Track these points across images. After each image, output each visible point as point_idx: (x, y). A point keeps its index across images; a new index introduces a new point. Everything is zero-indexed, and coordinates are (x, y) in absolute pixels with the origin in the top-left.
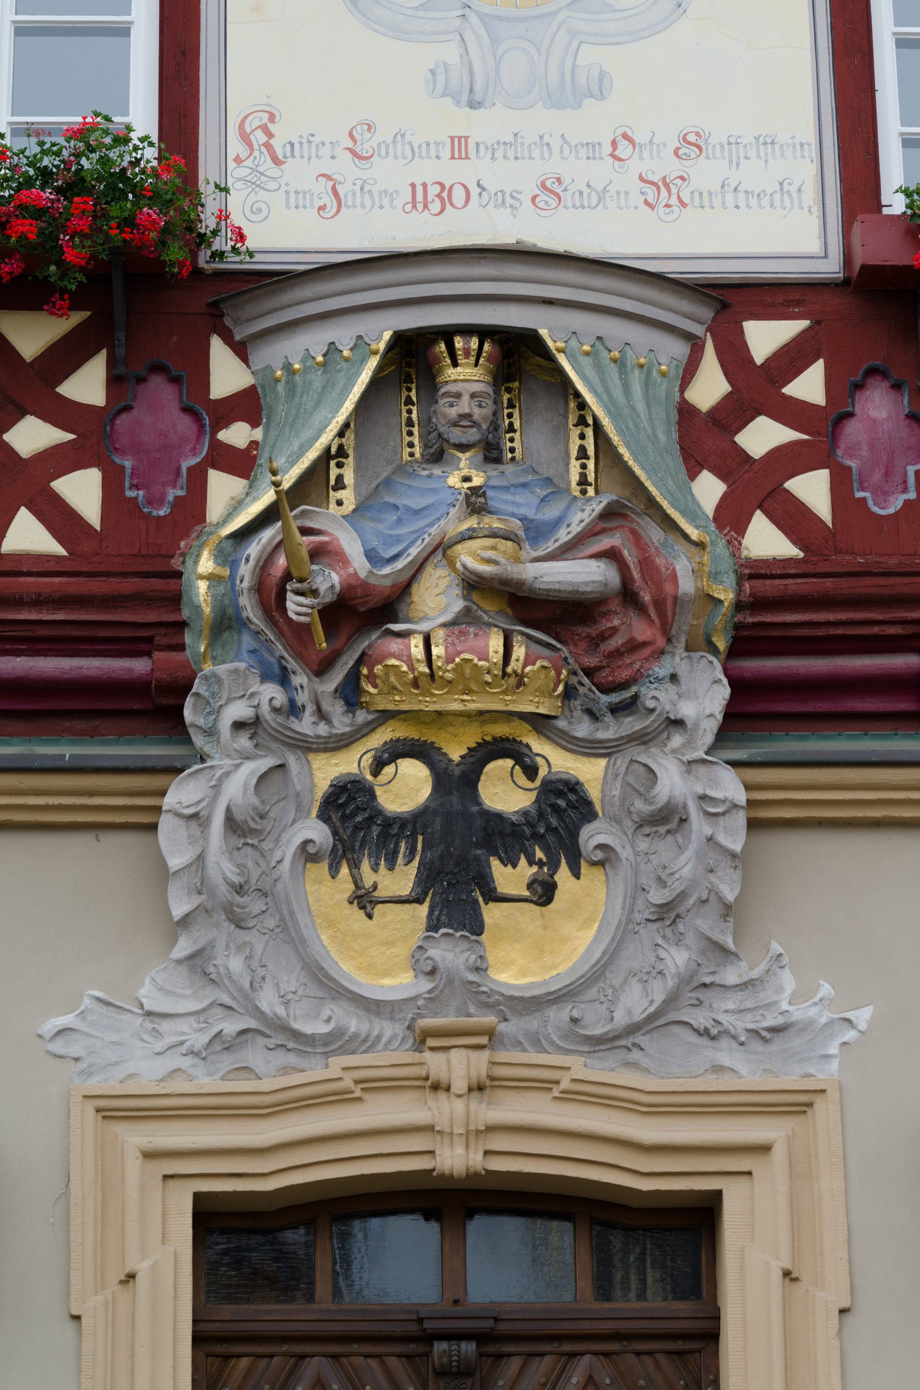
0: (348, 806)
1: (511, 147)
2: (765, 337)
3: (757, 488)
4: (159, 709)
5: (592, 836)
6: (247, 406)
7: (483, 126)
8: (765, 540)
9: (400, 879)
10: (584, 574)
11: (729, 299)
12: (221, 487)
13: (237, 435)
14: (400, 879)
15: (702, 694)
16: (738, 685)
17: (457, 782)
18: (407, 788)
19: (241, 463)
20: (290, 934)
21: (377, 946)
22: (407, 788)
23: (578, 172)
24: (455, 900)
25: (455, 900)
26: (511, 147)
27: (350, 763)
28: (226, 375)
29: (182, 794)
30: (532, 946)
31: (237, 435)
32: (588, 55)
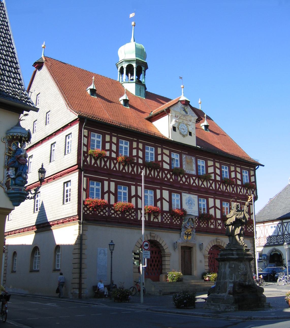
0: (185, 233)
1: (190, 211)
2: (197, 218)
3: (196, 224)
4: (181, 229)
5: (191, 235)
6: (183, 219)
7: (190, 210)
8: (196, 226)
9: (186, 236)
10: (193, 227)
11: (196, 217)
12: (183, 222)
13: (183, 220)
14: (186, 236)
15: (195, 231)
16: (196, 230)
17: (188, 233)
18: (187, 233)
19: (183, 221)
20: (184, 237)
21: (185, 238)
22: (187, 233)
23: (192, 212)
24: (188, 237)
25: (188, 237)
26: (190, 211)
27: (185, 232)
28: (183, 218)
29: (182, 233)
30: (190, 238)
31: (183, 220)
32: (192, 207)
